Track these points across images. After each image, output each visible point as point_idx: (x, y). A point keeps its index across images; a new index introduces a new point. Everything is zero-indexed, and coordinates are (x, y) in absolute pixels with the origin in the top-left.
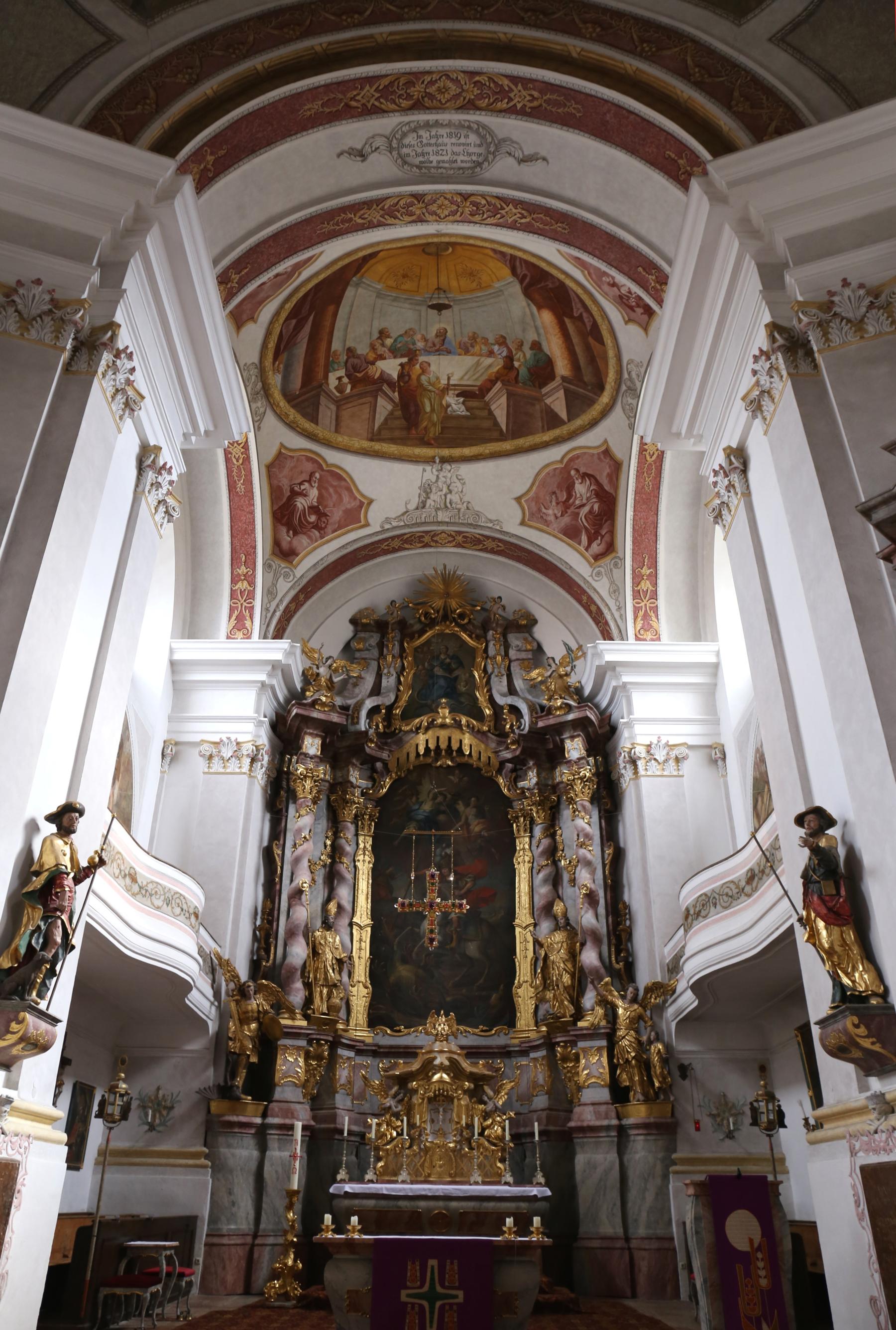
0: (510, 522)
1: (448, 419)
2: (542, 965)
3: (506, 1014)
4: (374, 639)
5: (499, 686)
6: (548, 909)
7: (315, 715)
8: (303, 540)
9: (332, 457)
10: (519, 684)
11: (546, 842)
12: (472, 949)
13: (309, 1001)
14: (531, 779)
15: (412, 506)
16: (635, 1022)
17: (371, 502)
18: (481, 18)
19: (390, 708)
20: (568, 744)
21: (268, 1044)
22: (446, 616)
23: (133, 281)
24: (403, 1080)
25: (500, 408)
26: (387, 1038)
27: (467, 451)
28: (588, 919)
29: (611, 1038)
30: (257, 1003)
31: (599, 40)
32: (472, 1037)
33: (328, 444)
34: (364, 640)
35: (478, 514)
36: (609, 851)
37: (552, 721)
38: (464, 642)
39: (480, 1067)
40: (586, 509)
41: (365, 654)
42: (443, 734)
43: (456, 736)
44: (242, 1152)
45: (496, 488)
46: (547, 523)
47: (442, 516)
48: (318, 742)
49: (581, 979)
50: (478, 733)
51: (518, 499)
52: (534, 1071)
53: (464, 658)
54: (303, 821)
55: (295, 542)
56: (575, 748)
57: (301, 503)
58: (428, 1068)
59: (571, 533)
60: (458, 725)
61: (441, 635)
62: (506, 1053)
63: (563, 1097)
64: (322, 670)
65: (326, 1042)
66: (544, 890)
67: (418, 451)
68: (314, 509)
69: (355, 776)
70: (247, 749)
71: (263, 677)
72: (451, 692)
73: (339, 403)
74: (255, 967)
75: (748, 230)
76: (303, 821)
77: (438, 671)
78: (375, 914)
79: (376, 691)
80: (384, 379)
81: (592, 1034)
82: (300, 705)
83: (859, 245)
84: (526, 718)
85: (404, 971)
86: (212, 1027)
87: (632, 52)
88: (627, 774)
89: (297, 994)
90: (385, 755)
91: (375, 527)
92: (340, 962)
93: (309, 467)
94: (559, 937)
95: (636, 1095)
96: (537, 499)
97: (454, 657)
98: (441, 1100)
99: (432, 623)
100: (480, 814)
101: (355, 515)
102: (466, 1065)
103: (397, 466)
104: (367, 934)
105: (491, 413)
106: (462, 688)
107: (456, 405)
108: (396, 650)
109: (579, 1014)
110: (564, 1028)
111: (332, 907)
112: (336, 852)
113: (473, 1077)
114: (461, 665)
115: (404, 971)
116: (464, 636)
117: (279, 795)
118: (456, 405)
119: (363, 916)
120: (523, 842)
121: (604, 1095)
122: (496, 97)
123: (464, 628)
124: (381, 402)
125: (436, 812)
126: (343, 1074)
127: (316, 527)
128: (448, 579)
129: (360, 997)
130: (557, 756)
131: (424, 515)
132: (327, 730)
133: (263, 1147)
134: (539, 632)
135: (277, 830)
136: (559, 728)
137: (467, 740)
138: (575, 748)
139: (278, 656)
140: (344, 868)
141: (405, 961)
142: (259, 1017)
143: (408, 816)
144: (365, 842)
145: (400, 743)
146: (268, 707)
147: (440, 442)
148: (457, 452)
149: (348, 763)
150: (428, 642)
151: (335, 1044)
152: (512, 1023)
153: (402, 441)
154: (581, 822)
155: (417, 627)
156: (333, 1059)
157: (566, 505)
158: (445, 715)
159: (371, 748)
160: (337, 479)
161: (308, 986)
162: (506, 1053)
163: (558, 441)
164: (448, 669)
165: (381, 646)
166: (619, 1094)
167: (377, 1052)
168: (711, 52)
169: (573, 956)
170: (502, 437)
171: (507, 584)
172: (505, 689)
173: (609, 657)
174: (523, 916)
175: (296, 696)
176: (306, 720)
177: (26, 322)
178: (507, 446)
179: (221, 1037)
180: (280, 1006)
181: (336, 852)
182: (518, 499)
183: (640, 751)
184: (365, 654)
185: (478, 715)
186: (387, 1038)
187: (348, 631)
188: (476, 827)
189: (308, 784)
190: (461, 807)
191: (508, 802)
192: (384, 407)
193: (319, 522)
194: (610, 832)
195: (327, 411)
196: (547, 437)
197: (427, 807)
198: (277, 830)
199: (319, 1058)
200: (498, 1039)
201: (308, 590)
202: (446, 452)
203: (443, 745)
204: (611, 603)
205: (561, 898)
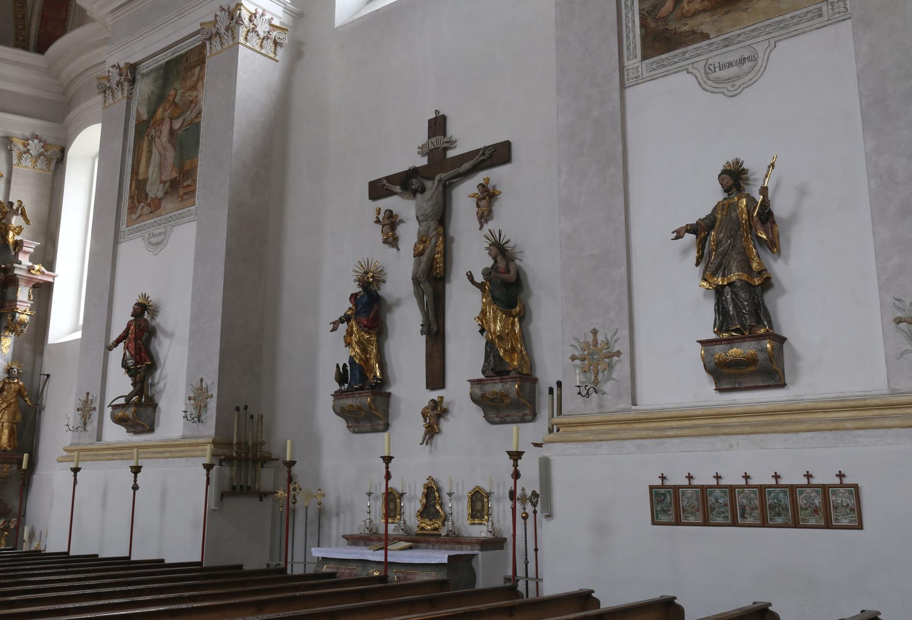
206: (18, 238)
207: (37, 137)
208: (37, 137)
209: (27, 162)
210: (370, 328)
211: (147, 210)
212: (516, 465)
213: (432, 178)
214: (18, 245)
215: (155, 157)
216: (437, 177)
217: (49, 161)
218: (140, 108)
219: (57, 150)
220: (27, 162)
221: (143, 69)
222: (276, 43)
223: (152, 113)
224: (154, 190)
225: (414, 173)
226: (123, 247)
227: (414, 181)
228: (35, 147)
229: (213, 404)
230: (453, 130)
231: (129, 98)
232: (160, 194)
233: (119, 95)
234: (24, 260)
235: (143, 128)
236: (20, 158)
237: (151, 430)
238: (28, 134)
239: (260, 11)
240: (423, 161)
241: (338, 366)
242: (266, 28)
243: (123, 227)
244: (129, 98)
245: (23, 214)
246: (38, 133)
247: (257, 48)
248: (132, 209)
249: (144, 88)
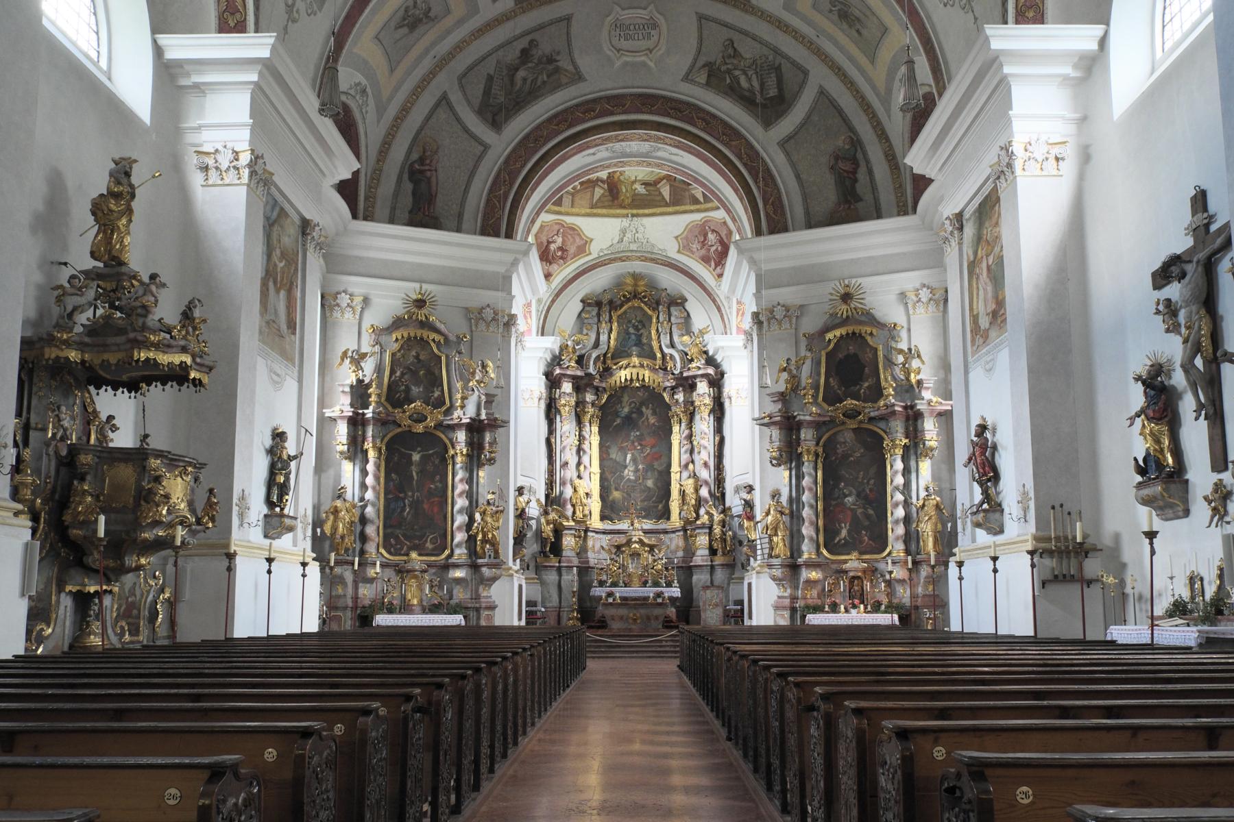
0: (672, 252)
1: (635, 195)
2: (683, 494)
3: (666, 514)
4: (595, 311)
5: (665, 340)
6: (686, 466)
7: (569, 372)
8: (555, 266)
9: (569, 220)
10: (676, 338)
11: (687, 432)
12: (650, 483)
13: (574, 513)
14: (680, 397)
15: (615, 241)
16: (723, 524)
17: (592, 240)
18: (651, 113)
19: (605, 355)
20: (699, 385)
21: (558, 532)
22: (635, 295)
23: (514, 277)
24: (618, 547)
25: (666, 191)
26: (608, 526)
27: (646, 211)
28: (704, 474)
29: (711, 528)
30: (553, 516)
31: (703, 130)
32: (648, 525)
33: (568, 214)
34: (589, 312)
35: (653, 246)
36: (717, 438)
37: (691, 373)
38: (645, 313)
39: (653, 541)
40: (713, 249)
41: (590, 321)
42: (635, 371)
43: (641, 372)
44: (552, 577)
45: (663, 231)
46: (693, 253)
47: (633, 247)
48: (570, 385)
49: (699, 502)
50: (653, 370)
51: (676, 238)
52: (677, 541)
53: (645, 322)
54: (566, 427)
55: (551, 269)
56: (702, 387)
57: (553, 247)
58: (629, 543)
59: (706, 260)
60: (642, 366)
61: (633, 307)
62: (665, 532)
63: (689, 552)
64: (569, 343)
65: (584, 532)
66: (685, 457)
67: (618, 211)
68: (560, 249)
69: (589, 397)
70: (537, 394)
71: (541, 355)
72: (639, 343)
73: (573, 195)
74: (547, 496)
75: (753, 262)
76: (566, 427)
77: (631, 330)
78: (602, 466)
79: (597, 344)
80: (599, 180)
81: (703, 526)
82: (561, 368)
83: (789, 285)
84: (679, 365)
85: (616, 495)
86: (534, 527)
87: (718, 139)
88: (727, 404)
89: (569, 512)
90: (604, 385)
91: (594, 255)
92: (587, 494)
93: (557, 227)
94: (691, 481)
95: (720, 552)
96: (687, 238)
97: (640, 322)
98: (635, 555)
99: (628, 300)
100: (654, 413)
101: (582, 250)
102: (646, 541)
103: (606, 220)
104: (598, 476)
105: (660, 193)
106: (644, 340)
107: (641, 189)
108: (607, 319)
109: (698, 517)
110: (691, 523)
111: (582, 468)
112: (581, 438)
113: (649, 546)
114: (644, 326)
115: (616, 495)
116: (646, 308)
117: (551, 410)
118: (641, 189)
119: (596, 468)
120: (676, 429)
121: (707, 552)
122: (658, 139)
123: (645, 303)
124: (597, 189)
125: (631, 412)
126: (590, 543)
127: (562, 258)
128: (636, 277)
129: (595, 505)
130: (693, 387)
131: (622, 247)
132: (574, 379)
133: (560, 575)
134: (688, 306)
135: (551, 430)
136: (695, 377)
137: (647, 373)
138: (702, 387)
139: (549, 345)
140: (586, 446)
141: (617, 489)
142: (554, 522)
143: (617, 414)
144: (595, 429)
145: (611, 375)
146: (542, 368)
147: (631, 206)
148: (641, 211)
149: (585, 391)
150: (625, 312)
151: (586, 531)
152: (668, 519)
153: (610, 207)
154: (704, 424)
155: (619, 302)
156: (586, 536)
157: (703, 244)
158: (635, 360)
159: (596, 383)
160: (573, 229)
161: (573, 506)
162: (665, 532)
163: (698, 211)
164: (637, 329)
165: (599, 315)
166: (713, 552)
167: (604, 532)
168: (752, 147)
169: (697, 491)
170: (667, 205)
171: (669, 280)
172: (668, 342)
173: (720, 344)
174: (675, 468)
175: (556, 360)
176: (564, 375)
177: (488, 325)
178: (670, 209)
179: (539, 532)
180: (563, 516)
181: (581, 438)
182: (676, 238)
183: (733, 394)
184: (590, 321)
185: (654, 357)
186: (608, 526)
187: (580, 306)
188: (652, 420)
189: (567, 408)
190: (644, 409)
191: (669, 407)
192: (598, 192)
193: (565, 254)
194: (719, 429)
195: (567, 201)
196: (692, 208)
197: (626, 410)
198: (551, 430)
199: (580, 537)
200: (662, 525)
201: (558, 295)
202: (635, 211)
203: (635, 377)
204: (726, 304)
205: (693, 462)
206: (918, 377)
207: (924, 286)
208: (924, 286)
209: (921, 309)
210: (1160, 419)
211: (981, 340)
212: (1151, 544)
213: (1190, 262)
214: (919, 382)
215: (981, 292)
216: (1195, 260)
217: (937, 303)
218: (968, 251)
219: (942, 292)
220: (921, 309)
221: (967, 215)
222: (1057, 159)
223: (976, 253)
224: (984, 322)
225: (1175, 260)
226: (972, 375)
227: (1173, 268)
228: (925, 294)
229: (1032, 504)
230: (1213, 206)
231: (960, 244)
232: (987, 326)
233: (953, 244)
234: (927, 395)
235: (972, 265)
236: (914, 308)
237: (1001, 531)
238: (918, 285)
239: (1034, 137)
240: (1189, 242)
241: (1135, 459)
242: (1045, 148)
243: (970, 359)
244: (960, 244)
245: (919, 356)
246: (926, 282)
247: (1038, 172)
248: (973, 341)
249: (969, 231)
